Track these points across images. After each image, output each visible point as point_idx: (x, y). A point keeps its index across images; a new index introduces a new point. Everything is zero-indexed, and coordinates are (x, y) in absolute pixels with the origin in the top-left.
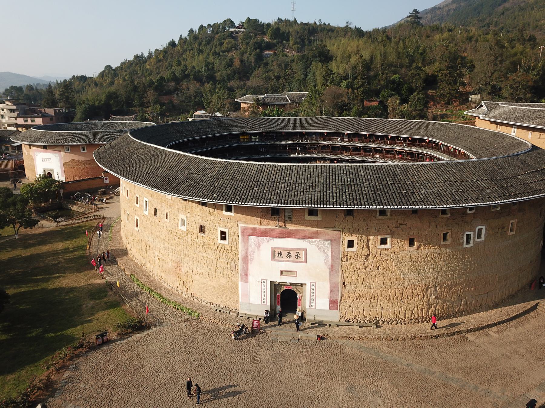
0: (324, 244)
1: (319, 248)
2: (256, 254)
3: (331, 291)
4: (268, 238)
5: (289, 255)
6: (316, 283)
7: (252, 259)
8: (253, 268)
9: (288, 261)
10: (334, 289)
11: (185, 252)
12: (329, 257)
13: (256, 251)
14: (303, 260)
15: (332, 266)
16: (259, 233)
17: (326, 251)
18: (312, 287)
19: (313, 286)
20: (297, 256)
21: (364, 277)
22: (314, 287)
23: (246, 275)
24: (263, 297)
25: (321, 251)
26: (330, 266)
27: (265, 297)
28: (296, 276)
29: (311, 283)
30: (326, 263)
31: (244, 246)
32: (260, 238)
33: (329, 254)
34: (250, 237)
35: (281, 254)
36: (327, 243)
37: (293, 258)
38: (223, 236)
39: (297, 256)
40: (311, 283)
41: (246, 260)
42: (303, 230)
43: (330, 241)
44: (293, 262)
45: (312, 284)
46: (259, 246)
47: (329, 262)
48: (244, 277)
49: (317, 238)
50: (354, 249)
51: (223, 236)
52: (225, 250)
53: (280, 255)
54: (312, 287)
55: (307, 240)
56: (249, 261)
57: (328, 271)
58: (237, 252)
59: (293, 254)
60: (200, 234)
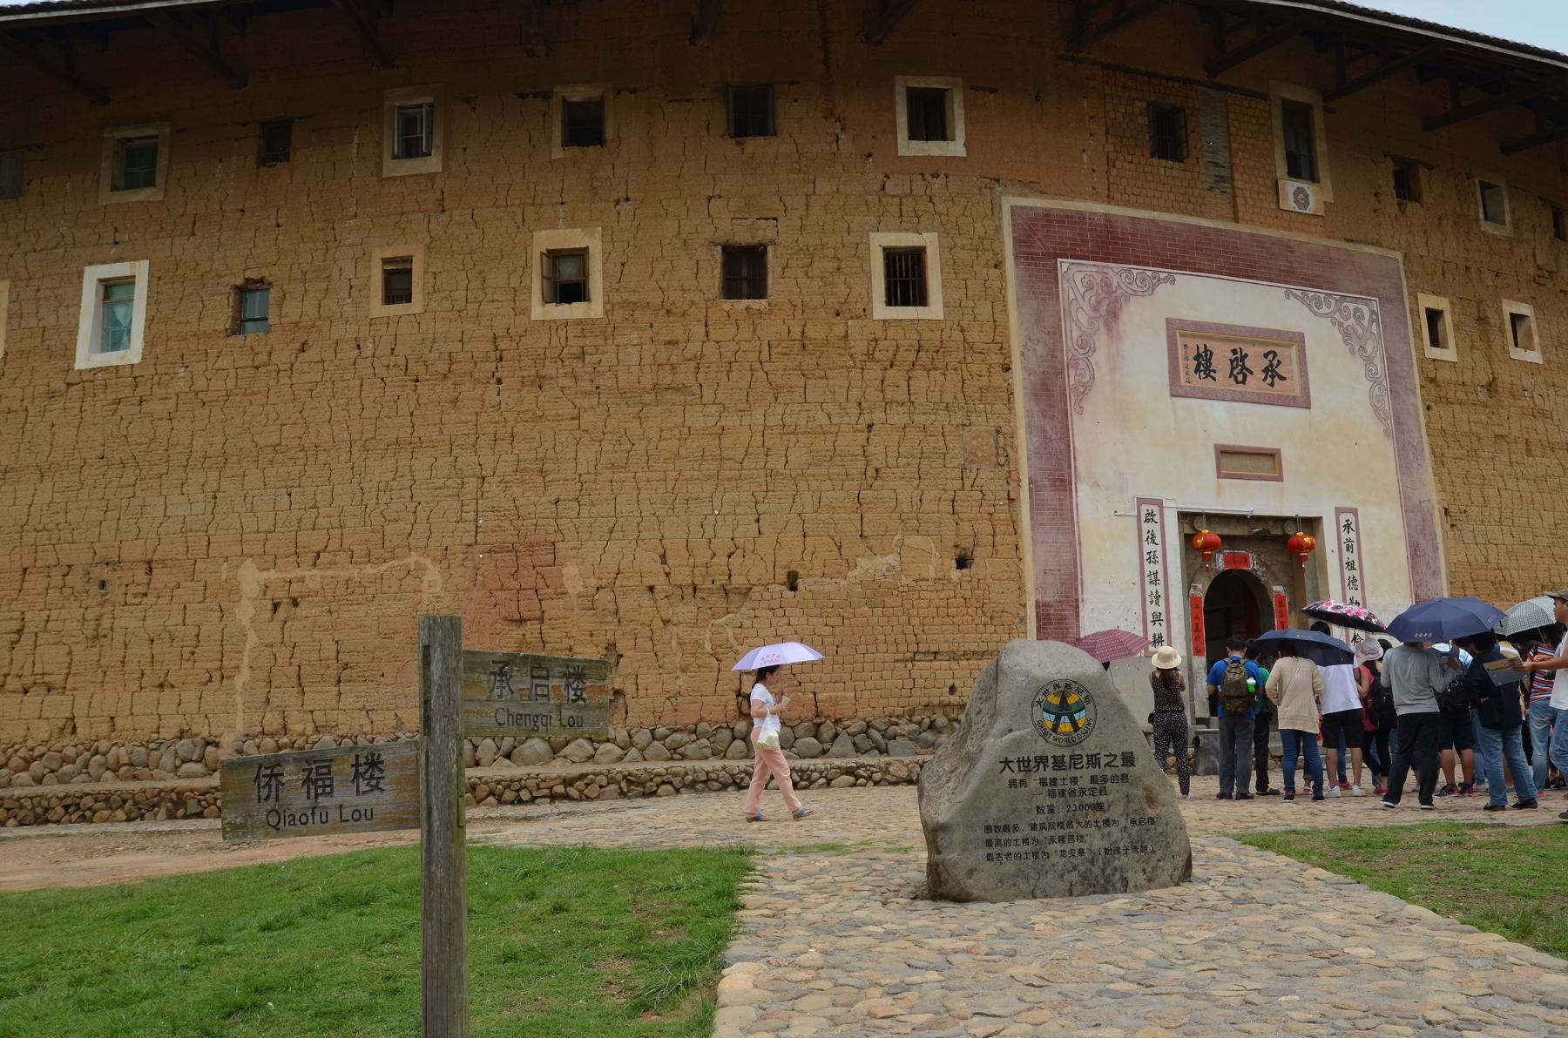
0: (1358, 316)
1: (1347, 335)
2: (1100, 358)
3: (1415, 553)
4: (1150, 271)
5: (1239, 366)
6: (1354, 512)
7: (1086, 389)
8: (1095, 439)
9: (1243, 398)
10: (1422, 543)
11: (587, 455)
13: (1101, 339)
14: (1297, 392)
15: (1398, 422)
16: (1107, 245)
17: (1369, 348)
18: (1345, 536)
19: (1348, 526)
20: (1271, 372)
21: (1502, 485)
22: (1352, 535)
23: (1059, 478)
24: (1151, 609)
25: (1352, 351)
26: (1391, 422)
27: (1162, 609)
28: (1280, 479)
29: (1339, 511)
30: (1376, 410)
31: (1039, 320)
32: (1116, 272)
33: (1380, 367)
34: (1064, 264)
35: (1209, 361)
36: (1365, 309)
37: (1255, 382)
38: (906, 278)
39: (1271, 372)
40: (1339, 511)
41: (1053, 396)
42: (1279, 242)
43: (1375, 306)
44: (1260, 400)
45: (1343, 518)
46: (1113, 314)
47: (1387, 403)
48: (1048, 495)
49: (1333, 285)
50: (1449, 354)
51: (906, 278)
52: (926, 353)
53: (1203, 363)
54: (1345, 536)
55: (1297, 290)
56: (1072, 400)
57: (1388, 448)
58: (997, 359)
60: (727, 305)
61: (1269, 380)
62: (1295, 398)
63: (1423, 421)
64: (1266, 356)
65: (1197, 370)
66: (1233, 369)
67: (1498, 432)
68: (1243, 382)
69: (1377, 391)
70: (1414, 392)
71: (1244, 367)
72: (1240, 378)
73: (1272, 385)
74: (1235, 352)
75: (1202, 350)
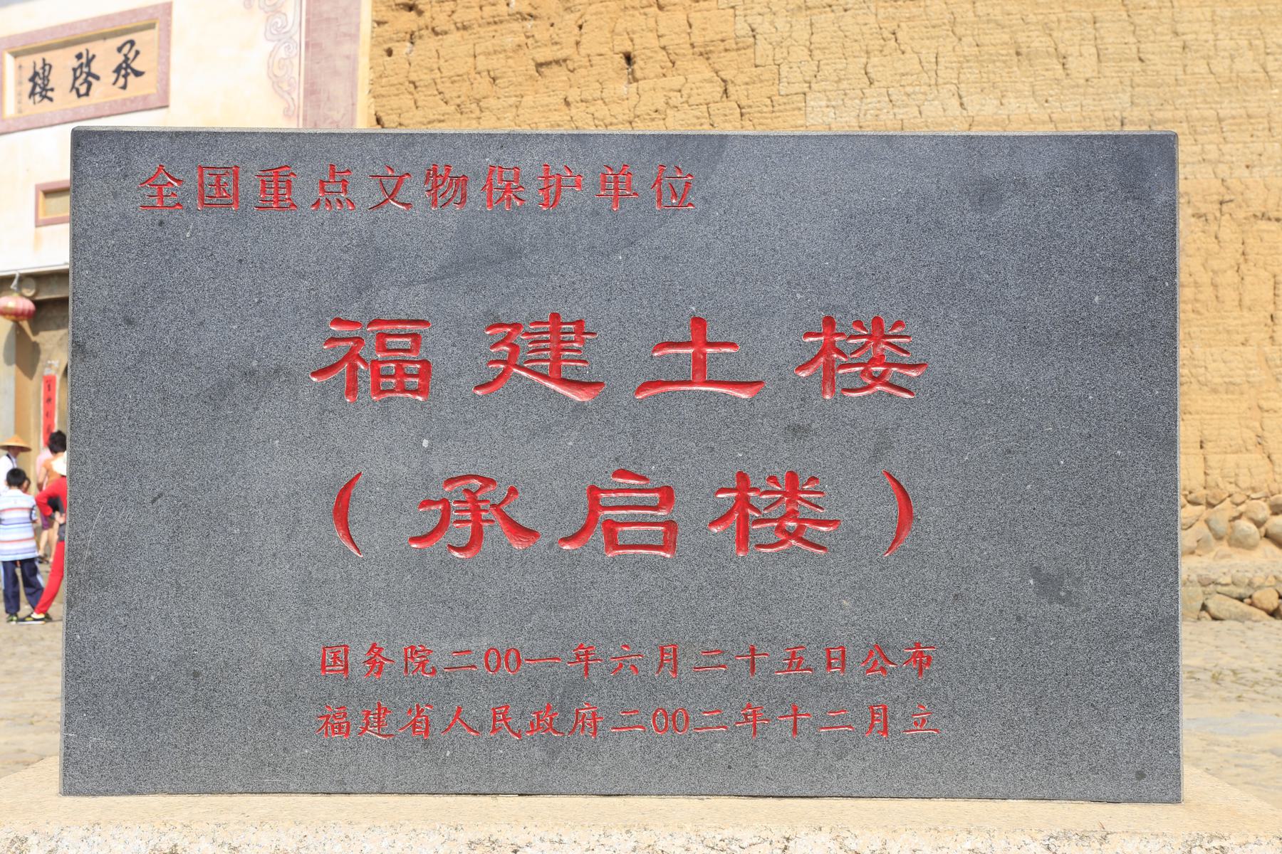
12: (299, 36)
20: (125, 70)
26: (298, 95)
30: (276, 82)
35: (46, 78)
59: (106, 57)
61: (121, 81)
62: (145, 98)
63: (364, 74)
64: (120, 50)
65: (32, 94)
66: (76, 79)
67: (544, 54)
68: (87, 94)
69: (282, 53)
70: (354, 37)
71: (89, 74)
72: (83, 89)
73: (124, 87)
74: (79, 56)
75: (40, 65)
